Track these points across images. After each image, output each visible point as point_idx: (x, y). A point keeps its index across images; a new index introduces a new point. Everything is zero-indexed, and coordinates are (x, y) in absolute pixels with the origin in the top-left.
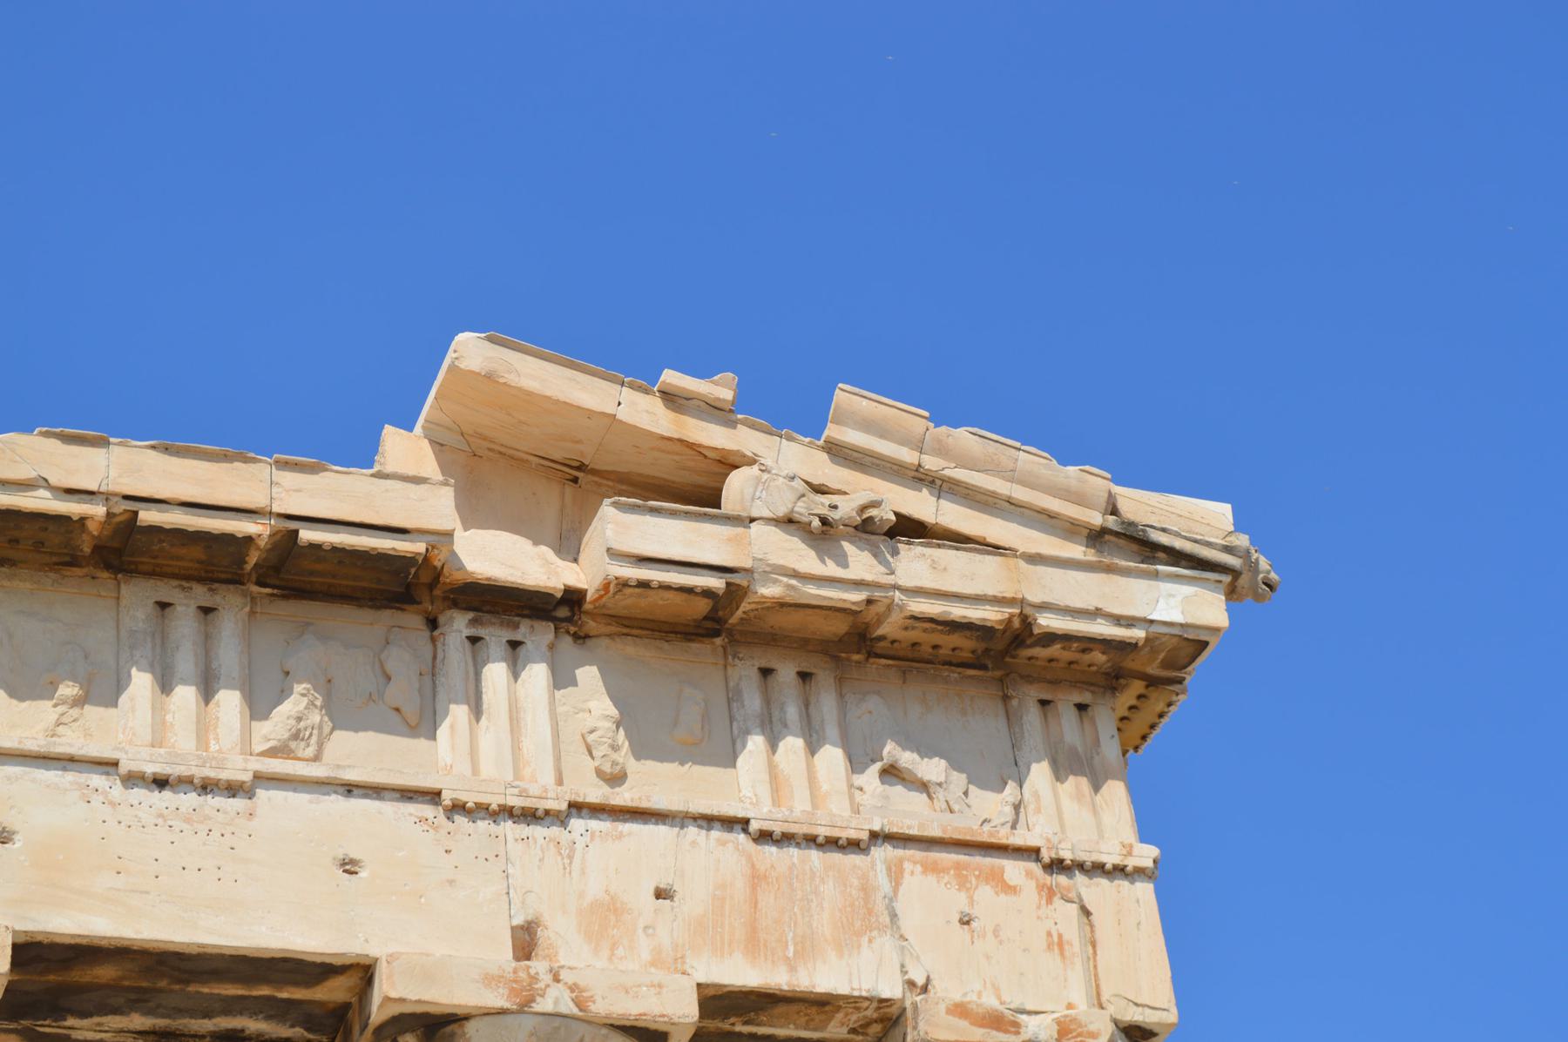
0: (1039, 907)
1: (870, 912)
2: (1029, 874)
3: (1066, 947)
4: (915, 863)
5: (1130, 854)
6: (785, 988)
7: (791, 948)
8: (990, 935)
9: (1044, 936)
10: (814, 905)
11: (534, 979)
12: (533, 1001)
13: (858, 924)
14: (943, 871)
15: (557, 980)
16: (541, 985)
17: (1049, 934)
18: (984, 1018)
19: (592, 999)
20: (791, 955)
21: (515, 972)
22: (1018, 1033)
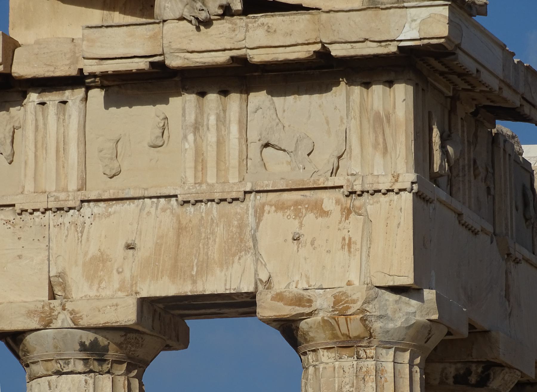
0: (340, 223)
1: (242, 240)
2: (338, 202)
3: (352, 246)
4: (271, 206)
5: (397, 181)
6: (189, 294)
7: (195, 269)
8: (309, 244)
9: (341, 239)
10: (210, 241)
11: (52, 310)
12: (51, 322)
13: (234, 249)
14: (288, 208)
15: (64, 309)
16: (56, 313)
17: (344, 239)
18: (292, 300)
19: (81, 318)
20: (194, 273)
21: (43, 307)
22: (311, 306)
